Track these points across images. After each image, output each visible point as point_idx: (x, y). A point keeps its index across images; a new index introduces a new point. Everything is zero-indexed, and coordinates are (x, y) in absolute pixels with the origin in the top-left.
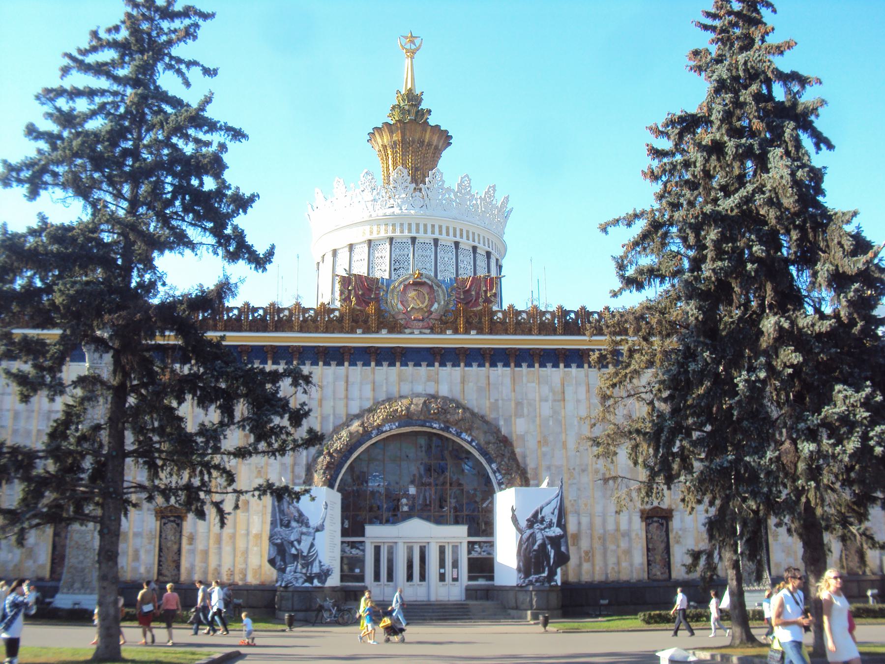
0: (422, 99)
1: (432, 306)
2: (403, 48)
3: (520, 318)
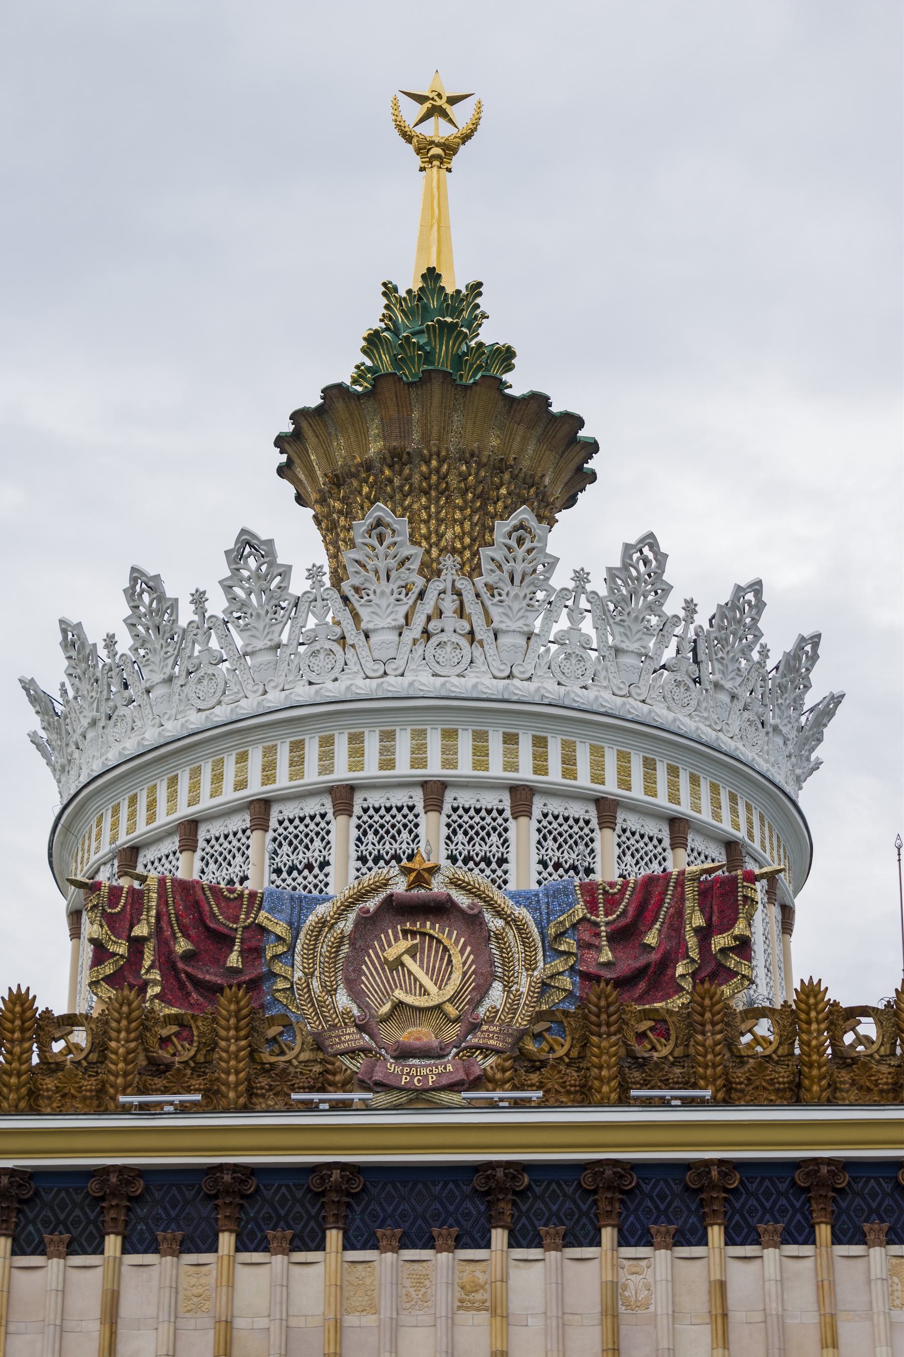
0: (475, 321)
1: (482, 991)
2: (408, 137)
3: (849, 1038)
